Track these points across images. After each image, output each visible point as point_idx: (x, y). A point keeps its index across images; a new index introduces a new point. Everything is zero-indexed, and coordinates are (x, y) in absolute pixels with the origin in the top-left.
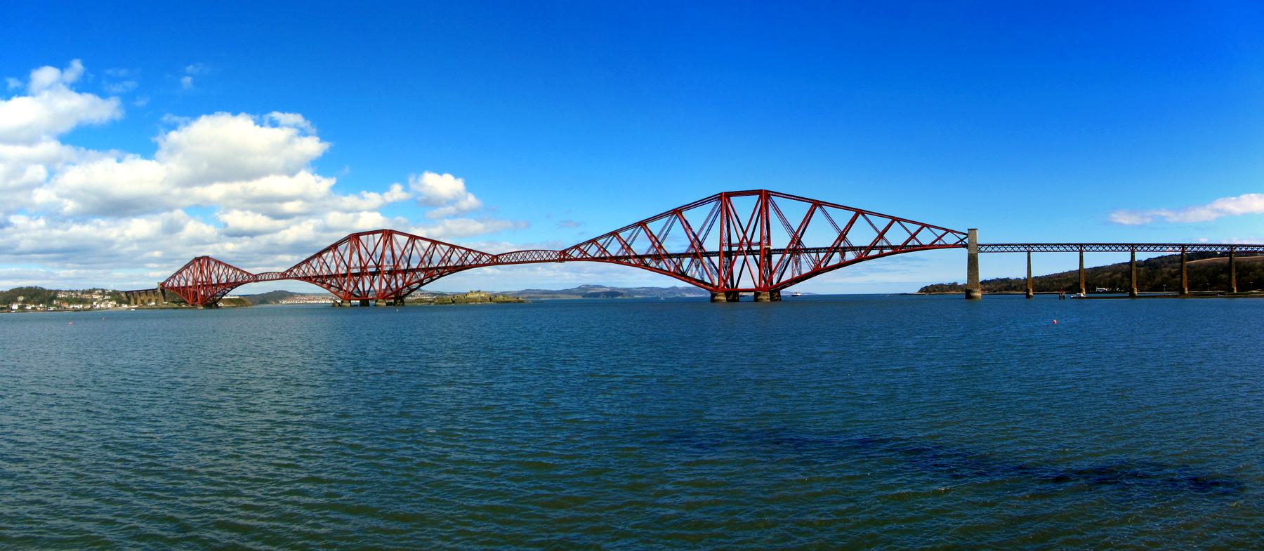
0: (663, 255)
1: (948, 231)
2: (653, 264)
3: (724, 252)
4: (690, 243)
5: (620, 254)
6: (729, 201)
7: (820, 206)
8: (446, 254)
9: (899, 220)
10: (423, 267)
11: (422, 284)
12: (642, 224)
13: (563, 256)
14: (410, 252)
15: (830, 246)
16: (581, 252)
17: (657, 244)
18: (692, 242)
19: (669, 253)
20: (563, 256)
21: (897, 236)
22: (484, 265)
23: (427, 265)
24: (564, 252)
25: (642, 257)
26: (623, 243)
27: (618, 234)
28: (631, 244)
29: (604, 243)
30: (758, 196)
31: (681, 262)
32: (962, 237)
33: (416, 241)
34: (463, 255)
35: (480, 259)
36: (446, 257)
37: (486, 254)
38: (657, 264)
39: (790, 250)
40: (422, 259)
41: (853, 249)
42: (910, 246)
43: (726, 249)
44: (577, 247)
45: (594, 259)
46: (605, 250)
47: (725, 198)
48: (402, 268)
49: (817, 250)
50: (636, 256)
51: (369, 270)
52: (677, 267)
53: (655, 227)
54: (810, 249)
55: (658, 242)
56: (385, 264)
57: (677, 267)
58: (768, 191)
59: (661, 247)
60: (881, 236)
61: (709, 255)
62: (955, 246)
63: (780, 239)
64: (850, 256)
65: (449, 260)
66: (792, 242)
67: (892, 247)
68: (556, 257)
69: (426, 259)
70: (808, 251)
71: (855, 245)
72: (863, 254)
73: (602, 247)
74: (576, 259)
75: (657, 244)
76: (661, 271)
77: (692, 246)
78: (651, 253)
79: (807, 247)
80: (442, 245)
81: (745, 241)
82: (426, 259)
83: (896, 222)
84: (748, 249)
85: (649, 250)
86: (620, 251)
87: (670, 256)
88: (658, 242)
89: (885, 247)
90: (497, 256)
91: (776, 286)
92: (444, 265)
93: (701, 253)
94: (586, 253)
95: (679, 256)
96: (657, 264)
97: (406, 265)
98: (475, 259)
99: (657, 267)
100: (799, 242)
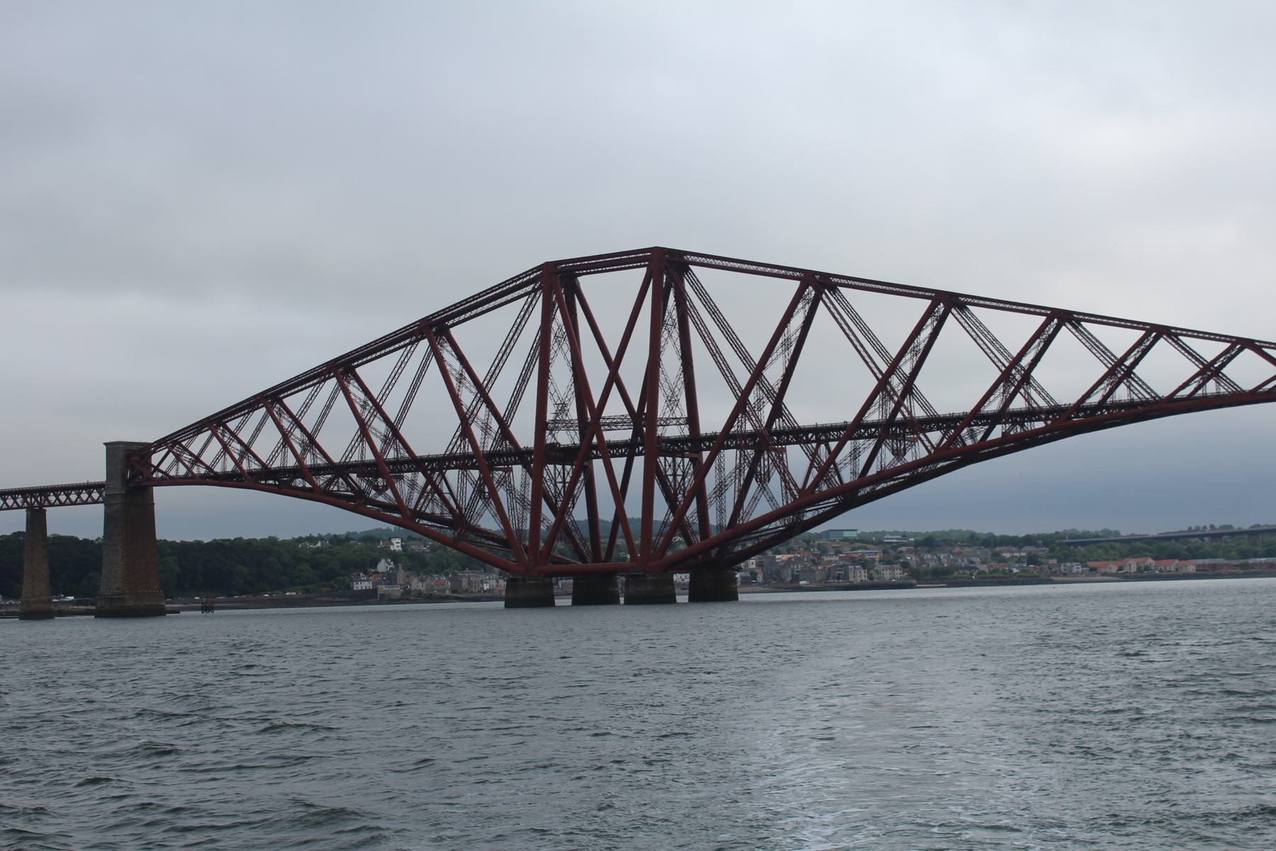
0: (397, 463)
1: (1239, 344)
4: (457, 421)
5: (277, 464)
6: (575, 290)
15: (850, 417)
16: (178, 458)
17: (378, 426)
18: (465, 421)
19: (419, 452)
29: (239, 428)
30: (638, 275)
39: (735, 436)
41: (935, 422)
43: (566, 438)
46: (247, 449)
49: (822, 433)
54: (806, 431)
55: (386, 419)
59: (394, 433)
61: (521, 456)
70: (799, 435)
71: (943, 410)
75: (378, 426)
77: (465, 432)
78: (356, 458)
81: (615, 408)
83: (1065, 333)
85: (351, 450)
87: (418, 464)
88: (386, 419)
89: (1031, 413)
94: (197, 460)
95: (433, 466)
99: (381, 499)
100: (778, 411)
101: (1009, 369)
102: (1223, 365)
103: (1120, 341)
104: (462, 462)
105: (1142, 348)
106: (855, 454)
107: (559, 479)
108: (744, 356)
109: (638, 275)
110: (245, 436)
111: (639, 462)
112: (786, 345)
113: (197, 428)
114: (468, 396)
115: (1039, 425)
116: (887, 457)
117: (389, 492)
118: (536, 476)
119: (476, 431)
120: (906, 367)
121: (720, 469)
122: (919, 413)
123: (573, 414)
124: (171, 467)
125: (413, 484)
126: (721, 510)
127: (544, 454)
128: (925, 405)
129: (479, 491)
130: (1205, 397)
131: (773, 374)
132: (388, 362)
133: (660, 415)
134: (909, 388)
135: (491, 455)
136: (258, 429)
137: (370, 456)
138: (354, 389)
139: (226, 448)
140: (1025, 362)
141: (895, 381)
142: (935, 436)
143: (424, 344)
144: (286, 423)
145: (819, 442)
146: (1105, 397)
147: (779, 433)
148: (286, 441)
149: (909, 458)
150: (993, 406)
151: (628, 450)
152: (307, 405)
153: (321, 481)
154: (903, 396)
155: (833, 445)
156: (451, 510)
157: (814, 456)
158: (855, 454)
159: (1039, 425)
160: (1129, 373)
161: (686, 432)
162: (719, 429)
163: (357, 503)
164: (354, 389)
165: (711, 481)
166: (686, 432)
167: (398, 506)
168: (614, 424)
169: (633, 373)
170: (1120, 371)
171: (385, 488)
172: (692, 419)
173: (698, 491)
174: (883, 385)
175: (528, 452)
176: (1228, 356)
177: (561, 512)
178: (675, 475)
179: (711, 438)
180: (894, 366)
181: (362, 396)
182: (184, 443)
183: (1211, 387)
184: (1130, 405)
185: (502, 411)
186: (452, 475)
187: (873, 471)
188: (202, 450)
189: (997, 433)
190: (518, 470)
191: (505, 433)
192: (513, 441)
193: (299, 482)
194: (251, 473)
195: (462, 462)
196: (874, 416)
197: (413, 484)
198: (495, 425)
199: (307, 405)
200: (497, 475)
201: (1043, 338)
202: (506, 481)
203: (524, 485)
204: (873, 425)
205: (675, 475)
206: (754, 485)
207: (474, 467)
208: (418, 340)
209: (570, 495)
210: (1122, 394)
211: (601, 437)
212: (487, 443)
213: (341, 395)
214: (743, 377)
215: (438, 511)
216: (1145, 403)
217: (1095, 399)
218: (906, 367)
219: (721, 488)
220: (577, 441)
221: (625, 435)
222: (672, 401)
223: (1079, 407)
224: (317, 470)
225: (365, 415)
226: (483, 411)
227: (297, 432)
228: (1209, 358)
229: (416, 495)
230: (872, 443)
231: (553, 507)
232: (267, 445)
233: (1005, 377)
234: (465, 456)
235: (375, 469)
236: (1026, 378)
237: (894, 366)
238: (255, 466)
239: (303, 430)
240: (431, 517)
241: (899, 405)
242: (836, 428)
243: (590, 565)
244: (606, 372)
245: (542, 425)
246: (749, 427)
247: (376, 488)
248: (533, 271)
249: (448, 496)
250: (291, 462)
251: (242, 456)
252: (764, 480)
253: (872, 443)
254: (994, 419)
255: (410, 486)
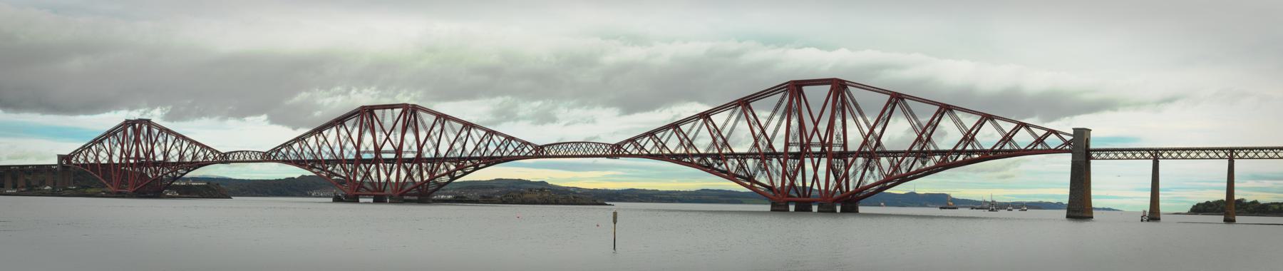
0: (726, 154)
2: (716, 166)
3: (794, 153)
4: (753, 140)
5: (678, 152)
6: (801, 92)
7: (902, 99)
8: (482, 140)
9: (991, 118)
10: (452, 156)
11: (453, 178)
12: (706, 116)
13: (616, 151)
14: (438, 135)
16: (636, 147)
17: (720, 140)
18: (756, 140)
20: (616, 151)
21: (988, 137)
22: (526, 157)
23: (459, 152)
24: (619, 146)
25: (704, 156)
26: (682, 136)
27: (679, 127)
28: (694, 138)
29: (662, 137)
30: (829, 87)
31: (746, 162)
32: (1068, 138)
33: (446, 122)
34: (502, 143)
35: (523, 150)
36: (482, 145)
37: (529, 143)
38: (720, 165)
39: (862, 153)
40: (452, 146)
42: (1006, 151)
43: (795, 149)
44: (632, 140)
45: (650, 156)
46: (664, 145)
47: (795, 89)
48: (427, 155)
50: (699, 155)
51: (384, 156)
52: (741, 167)
53: (718, 119)
54: (888, 152)
55: (722, 137)
56: (405, 148)
57: (741, 167)
58: (844, 81)
60: (969, 137)
61: (777, 155)
62: (1056, 151)
63: (855, 139)
64: (930, 163)
65: (487, 149)
66: (865, 142)
67: (985, 151)
68: (608, 151)
69: (458, 145)
70: (886, 154)
72: (948, 161)
73: (660, 140)
74: (630, 155)
75: (720, 140)
76: (721, 173)
77: (756, 145)
78: (710, 152)
79: (888, 149)
80: (479, 131)
81: (815, 139)
82: (458, 145)
83: (988, 122)
84: (822, 150)
85: (709, 149)
86: (678, 147)
87: (735, 155)
88: (722, 137)
89: (974, 152)
90: (542, 147)
91: (853, 193)
92: (478, 155)
93: (770, 154)
94: (643, 148)
95: (744, 156)
96: (720, 165)
97: (433, 152)
98: (516, 150)
99: (720, 168)
100: (878, 144)
101: (967, 135)
102: (1045, 139)
103: (1008, 127)
104: (754, 156)
105: (1016, 130)
106: (907, 162)
107: (792, 165)
108: (867, 123)
109: (829, 87)
110: (663, 140)
111: (824, 162)
112: (883, 119)
113: (644, 136)
114: (757, 131)
115: (976, 156)
116: (918, 165)
117: (724, 166)
118: (784, 165)
119: (761, 147)
120: (928, 131)
121: (856, 165)
122: (932, 148)
123: (798, 140)
124: (632, 151)
125: (733, 164)
126: (855, 181)
127: (786, 155)
128: (935, 146)
129: (759, 165)
130: (1037, 150)
131: (877, 130)
132: (726, 114)
133: (834, 143)
134: (929, 139)
135: (765, 154)
136: (669, 138)
137: (716, 151)
138: (710, 124)
139: (656, 144)
140: (973, 132)
141: (924, 136)
142: (938, 158)
143: (740, 107)
144: (682, 136)
145: (894, 157)
146: (1001, 147)
147: (878, 152)
148: (682, 143)
149: (927, 165)
150: (960, 148)
151: (820, 155)
152: (690, 130)
153: (695, 160)
154: (926, 142)
155: (900, 158)
156: (747, 174)
157: (892, 163)
158: (907, 162)
159: (976, 156)
160: (1010, 139)
161: (842, 150)
162: (856, 149)
163: (709, 169)
164: (710, 124)
165: (851, 170)
166: (842, 150)
167: (727, 172)
168: (815, 145)
169: (823, 127)
170: (1007, 138)
171: (722, 164)
172: (845, 145)
173: (846, 175)
174: (920, 138)
175: (780, 153)
176: (1046, 136)
177: (793, 179)
178: (838, 166)
179: (853, 153)
180: (924, 131)
181: (713, 127)
182: (638, 141)
183: (1039, 147)
184: (1010, 151)
185: (769, 137)
186: (750, 162)
187: (914, 169)
188: (645, 144)
189: (961, 158)
190: (775, 161)
191: (770, 146)
192: (773, 149)
193: (686, 160)
194: (667, 155)
195: (754, 156)
196: (916, 148)
197: (733, 164)
198: (767, 142)
199: (690, 130)
200: (767, 161)
201: (980, 124)
202: (771, 164)
203: (778, 166)
204: (915, 152)
205: (838, 166)
206: (868, 171)
207: (758, 158)
208: (738, 106)
209: (796, 173)
210: (1007, 147)
211: (810, 150)
212: (763, 148)
213: (705, 125)
214: (867, 131)
215: (743, 175)
216: (1015, 150)
217: (997, 148)
218: (928, 131)
219: (855, 173)
220: (799, 150)
221: (818, 149)
222: (838, 137)
223: (992, 150)
224: (693, 155)
225: (715, 135)
226: (763, 138)
227: (686, 140)
228: (1040, 136)
229: (735, 168)
230: (914, 158)
231: (790, 179)
232: (673, 145)
233: (965, 138)
234: (756, 154)
235: (716, 157)
236: (973, 139)
237: (924, 131)
238: (667, 152)
239: (688, 139)
240: (741, 177)
241: (925, 145)
242: (901, 152)
243: (802, 199)
244: (813, 126)
245: (787, 145)
246: (868, 150)
247: (718, 164)
248: (786, 83)
249: (746, 169)
250: (683, 151)
251: (662, 147)
252: (872, 170)
253: (914, 158)
254: (960, 152)
255: (732, 165)
